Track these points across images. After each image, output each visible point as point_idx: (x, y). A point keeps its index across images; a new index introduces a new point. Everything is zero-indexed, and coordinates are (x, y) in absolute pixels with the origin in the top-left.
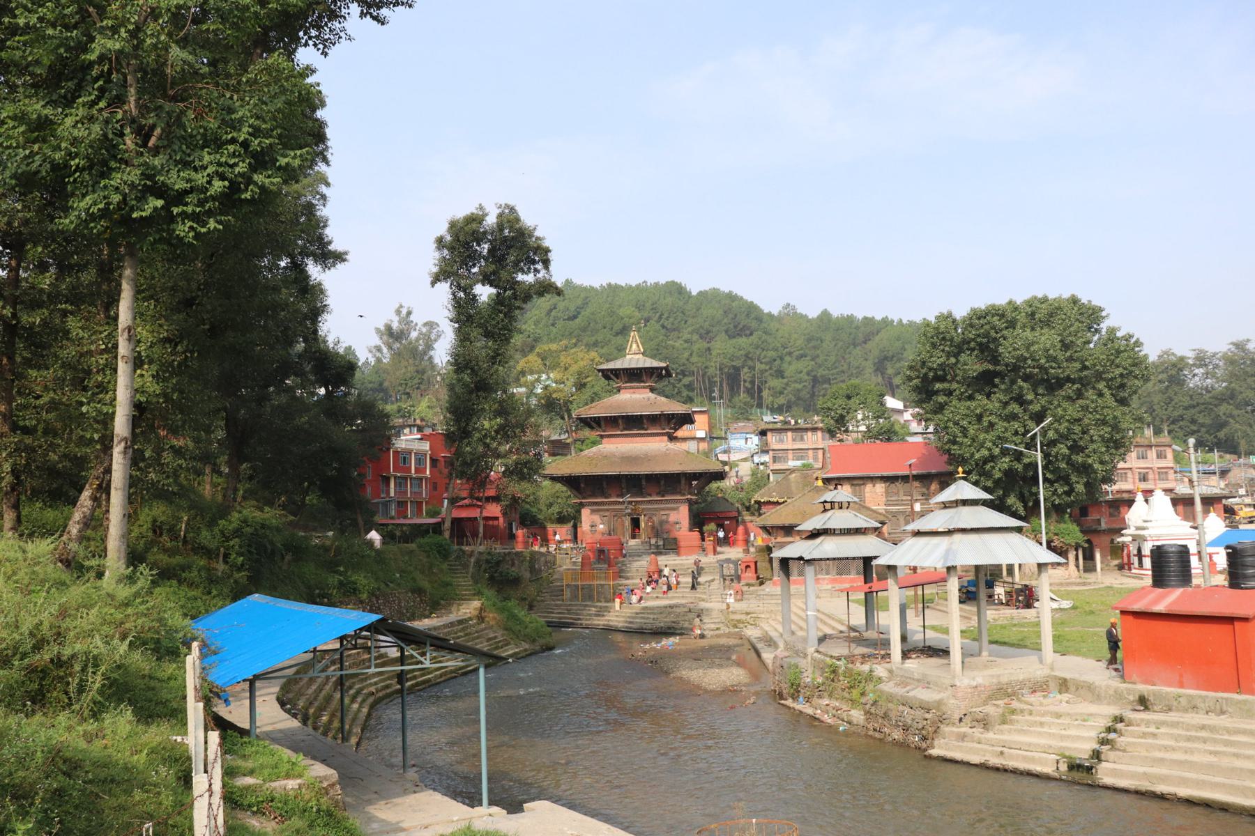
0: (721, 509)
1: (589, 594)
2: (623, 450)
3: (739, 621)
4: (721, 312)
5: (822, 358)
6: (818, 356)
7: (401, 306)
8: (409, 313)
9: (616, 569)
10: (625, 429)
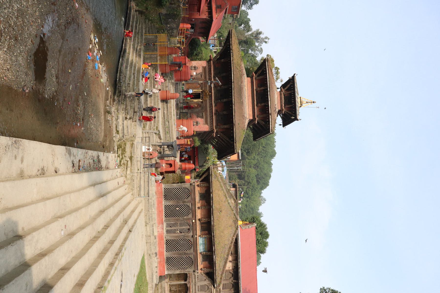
0: (200, 158)
1: (149, 46)
2: (244, 89)
3: (124, 150)
4: (266, 172)
5: (246, 214)
6: (246, 213)
7: (269, 39)
8: (266, 42)
9: (168, 69)
10: (257, 92)
